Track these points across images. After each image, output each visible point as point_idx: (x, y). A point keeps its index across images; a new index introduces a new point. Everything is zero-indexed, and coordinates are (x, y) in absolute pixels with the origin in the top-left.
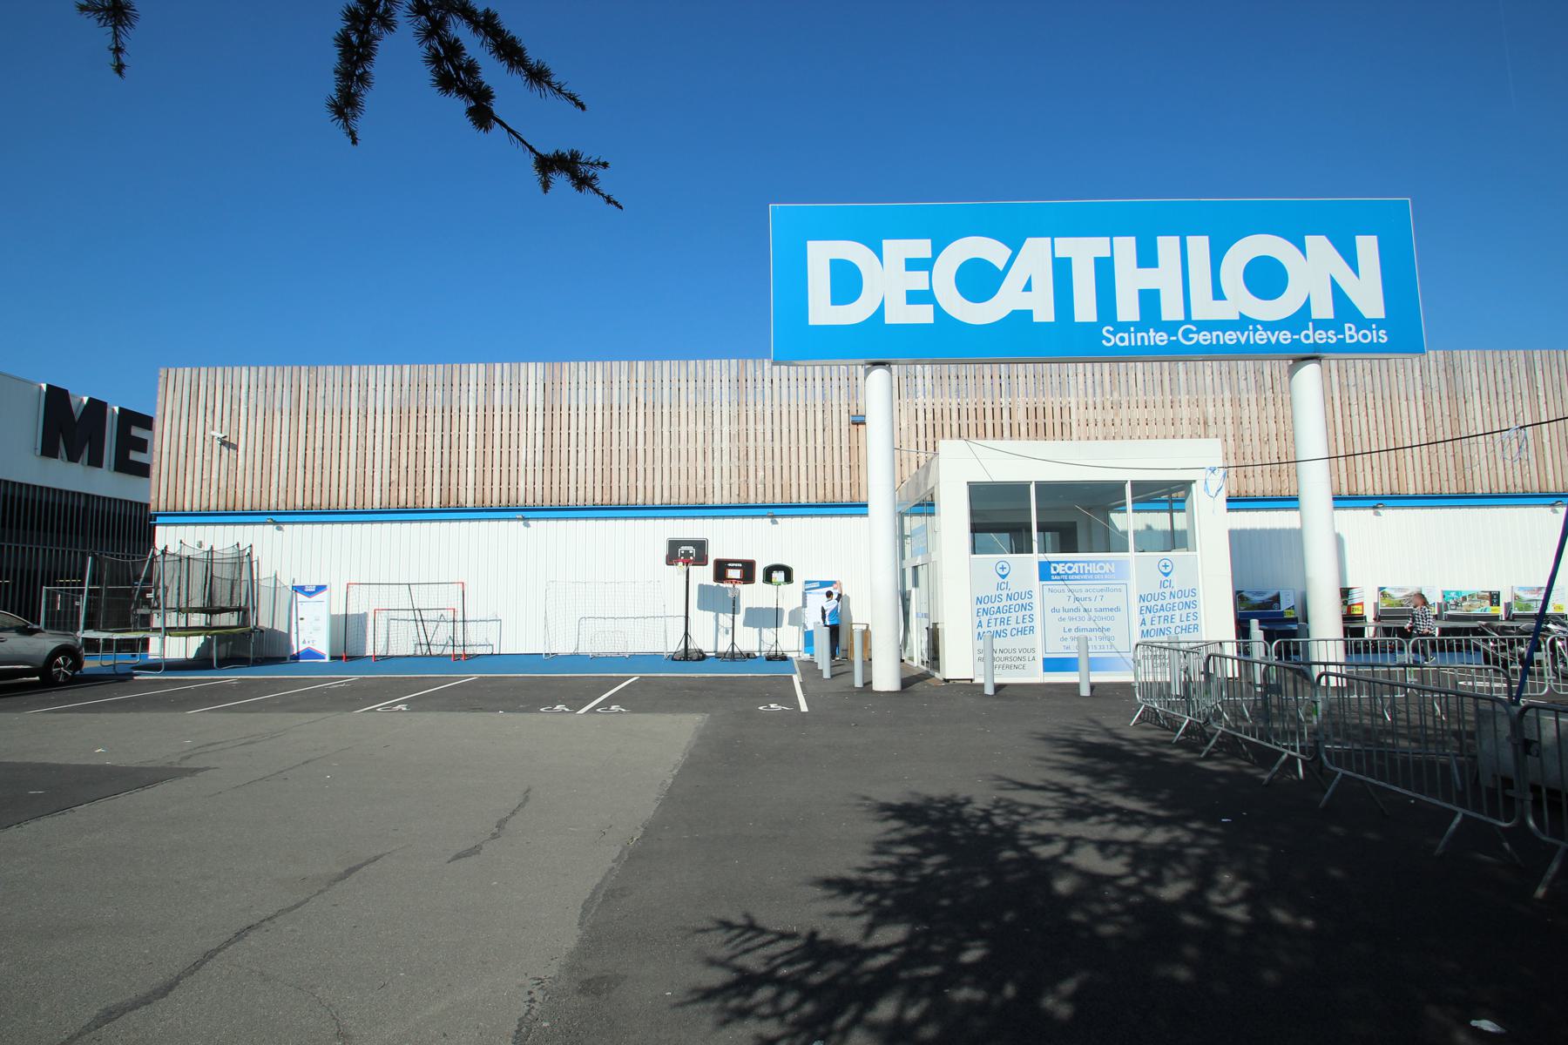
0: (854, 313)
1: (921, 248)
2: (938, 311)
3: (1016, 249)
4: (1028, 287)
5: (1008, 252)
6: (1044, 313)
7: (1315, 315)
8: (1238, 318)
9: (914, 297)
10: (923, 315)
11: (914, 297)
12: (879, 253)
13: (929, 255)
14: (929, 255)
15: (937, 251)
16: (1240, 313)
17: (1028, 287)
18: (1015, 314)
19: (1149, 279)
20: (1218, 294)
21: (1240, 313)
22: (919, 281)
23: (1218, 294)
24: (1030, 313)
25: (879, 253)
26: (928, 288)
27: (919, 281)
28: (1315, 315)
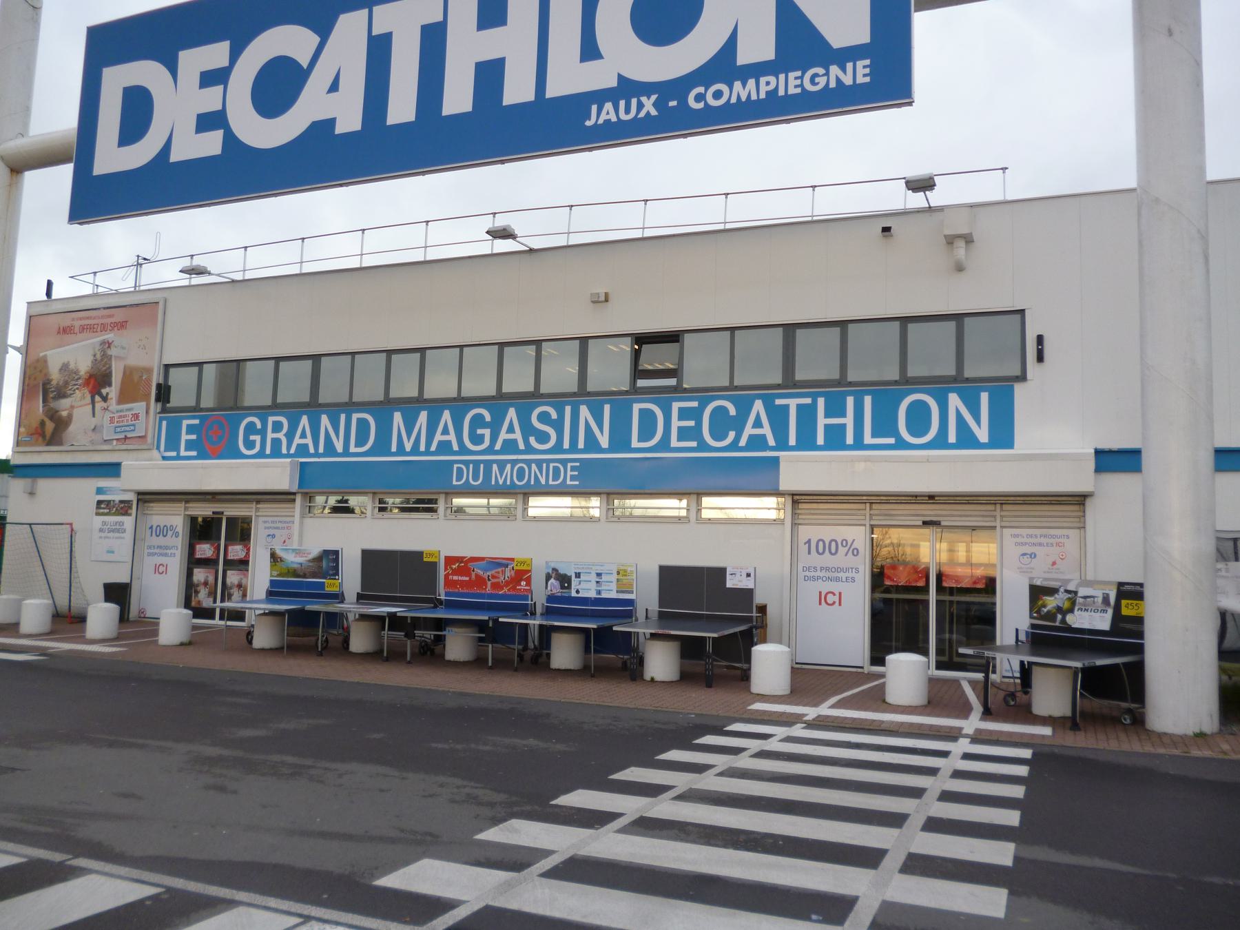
0: (140, 154)
1: (215, 54)
2: (230, 140)
3: (324, 31)
4: (334, 87)
5: (316, 39)
6: (350, 120)
7: (744, 57)
8: (614, 84)
9: (210, 121)
10: (212, 144)
11: (210, 121)
12: (173, 70)
13: (225, 62)
14: (225, 62)
15: (235, 55)
16: (620, 76)
17: (334, 87)
18: (315, 125)
19: (491, 44)
20: (590, 51)
21: (620, 76)
22: (210, 100)
23: (590, 51)
24: (332, 122)
25: (173, 70)
26: (220, 108)
27: (210, 100)
28: (744, 57)
